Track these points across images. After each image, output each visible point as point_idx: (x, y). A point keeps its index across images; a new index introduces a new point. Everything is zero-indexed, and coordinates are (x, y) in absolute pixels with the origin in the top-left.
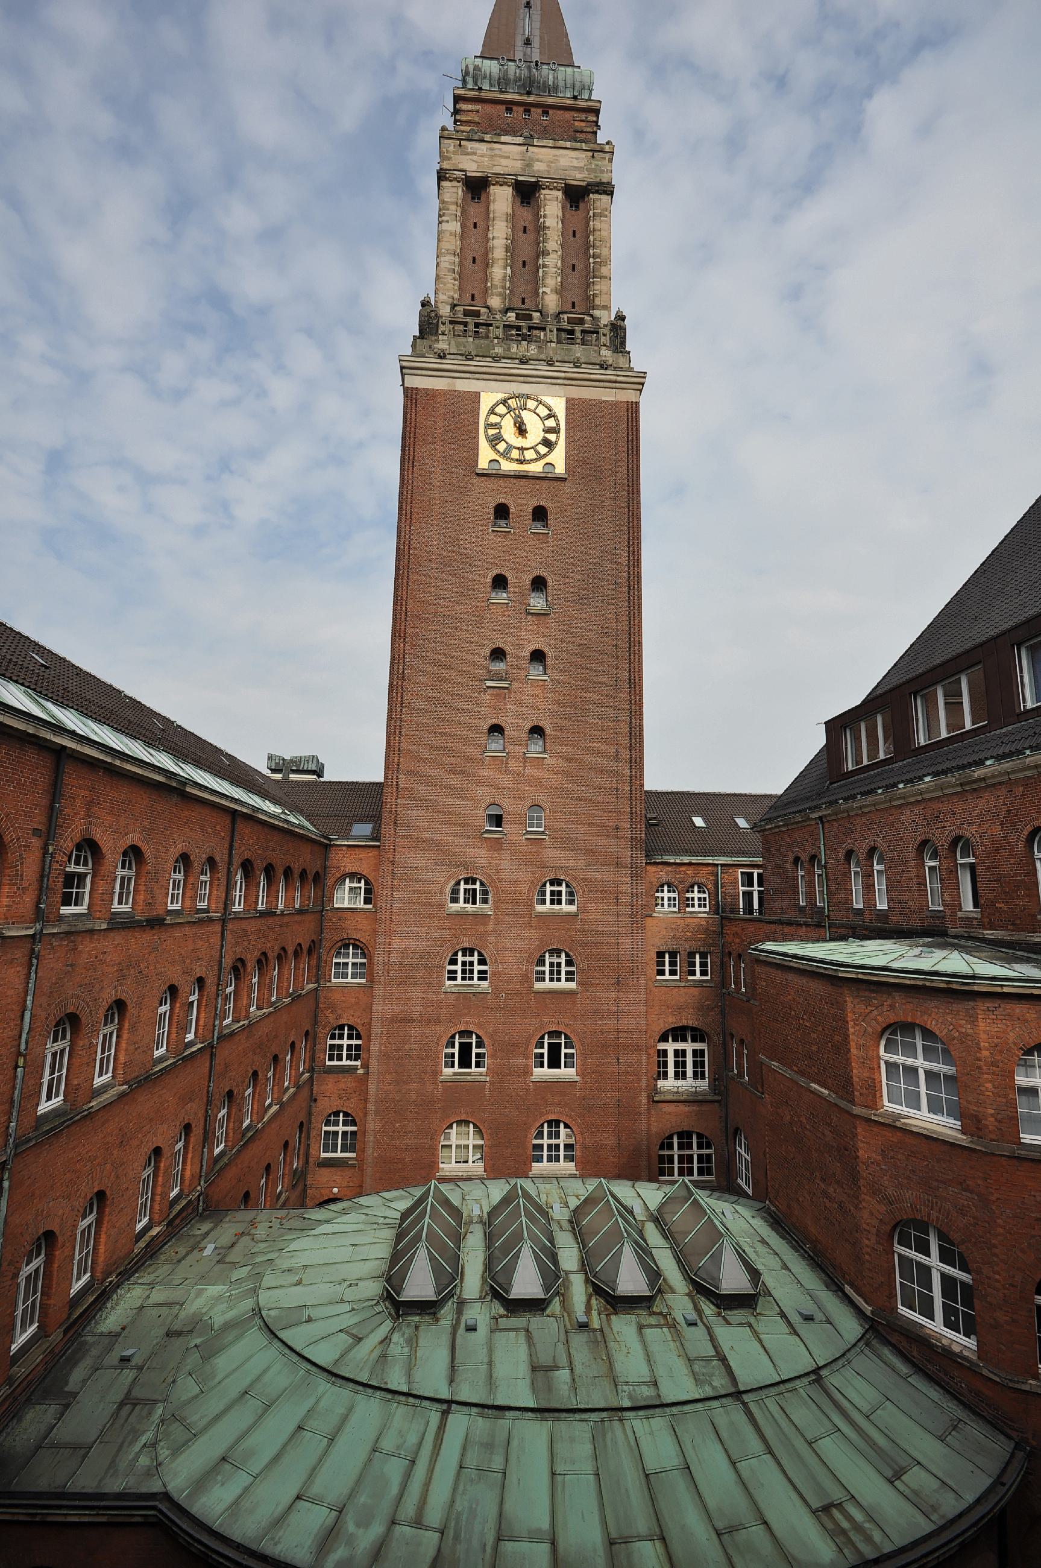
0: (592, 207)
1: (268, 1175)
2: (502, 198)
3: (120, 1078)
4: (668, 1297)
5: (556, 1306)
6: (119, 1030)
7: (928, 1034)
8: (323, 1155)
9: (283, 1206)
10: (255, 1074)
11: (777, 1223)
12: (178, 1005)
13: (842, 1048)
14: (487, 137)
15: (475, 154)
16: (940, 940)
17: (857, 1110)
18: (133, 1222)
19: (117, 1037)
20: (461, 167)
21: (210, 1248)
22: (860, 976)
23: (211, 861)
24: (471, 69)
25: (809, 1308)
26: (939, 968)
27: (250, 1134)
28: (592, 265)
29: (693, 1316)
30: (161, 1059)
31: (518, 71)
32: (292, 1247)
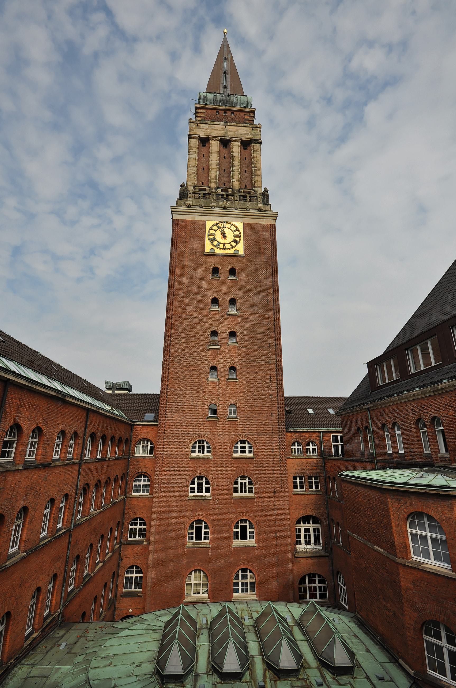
0: (253, 148)
1: (95, 602)
2: (215, 146)
3: (22, 549)
4: (307, 669)
5: (247, 677)
6: (24, 523)
7: (430, 518)
8: (125, 590)
9: (103, 620)
10: (91, 545)
11: (362, 624)
12: (54, 509)
13: (388, 527)
14: (209, 122)
15: (204, 129)
16: (431, 469)
17: (398, 560)
18: (24, 630)
19: (22, 526)
20: (198, 133)
21: (63, 645)
22: (394, 488)
23: (76, 434)
24: (202, 97)
25: (381, 673)
26: (431, 483)
27: (87, 579)
28: (253, 171)
29: (320, 680)
30: (44, 538)
31: (221, 98)
32: (107, 644)
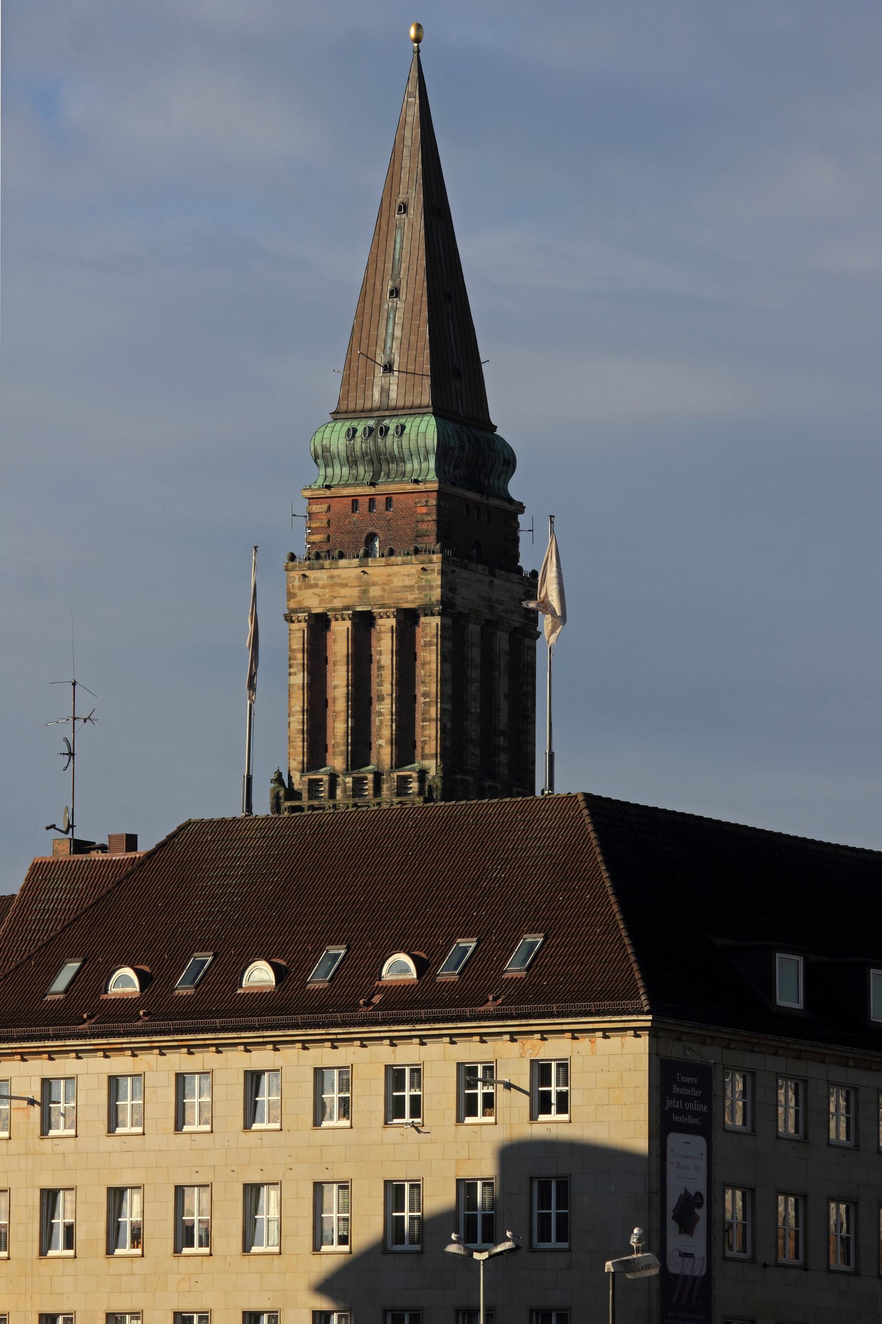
15: (316, 586)
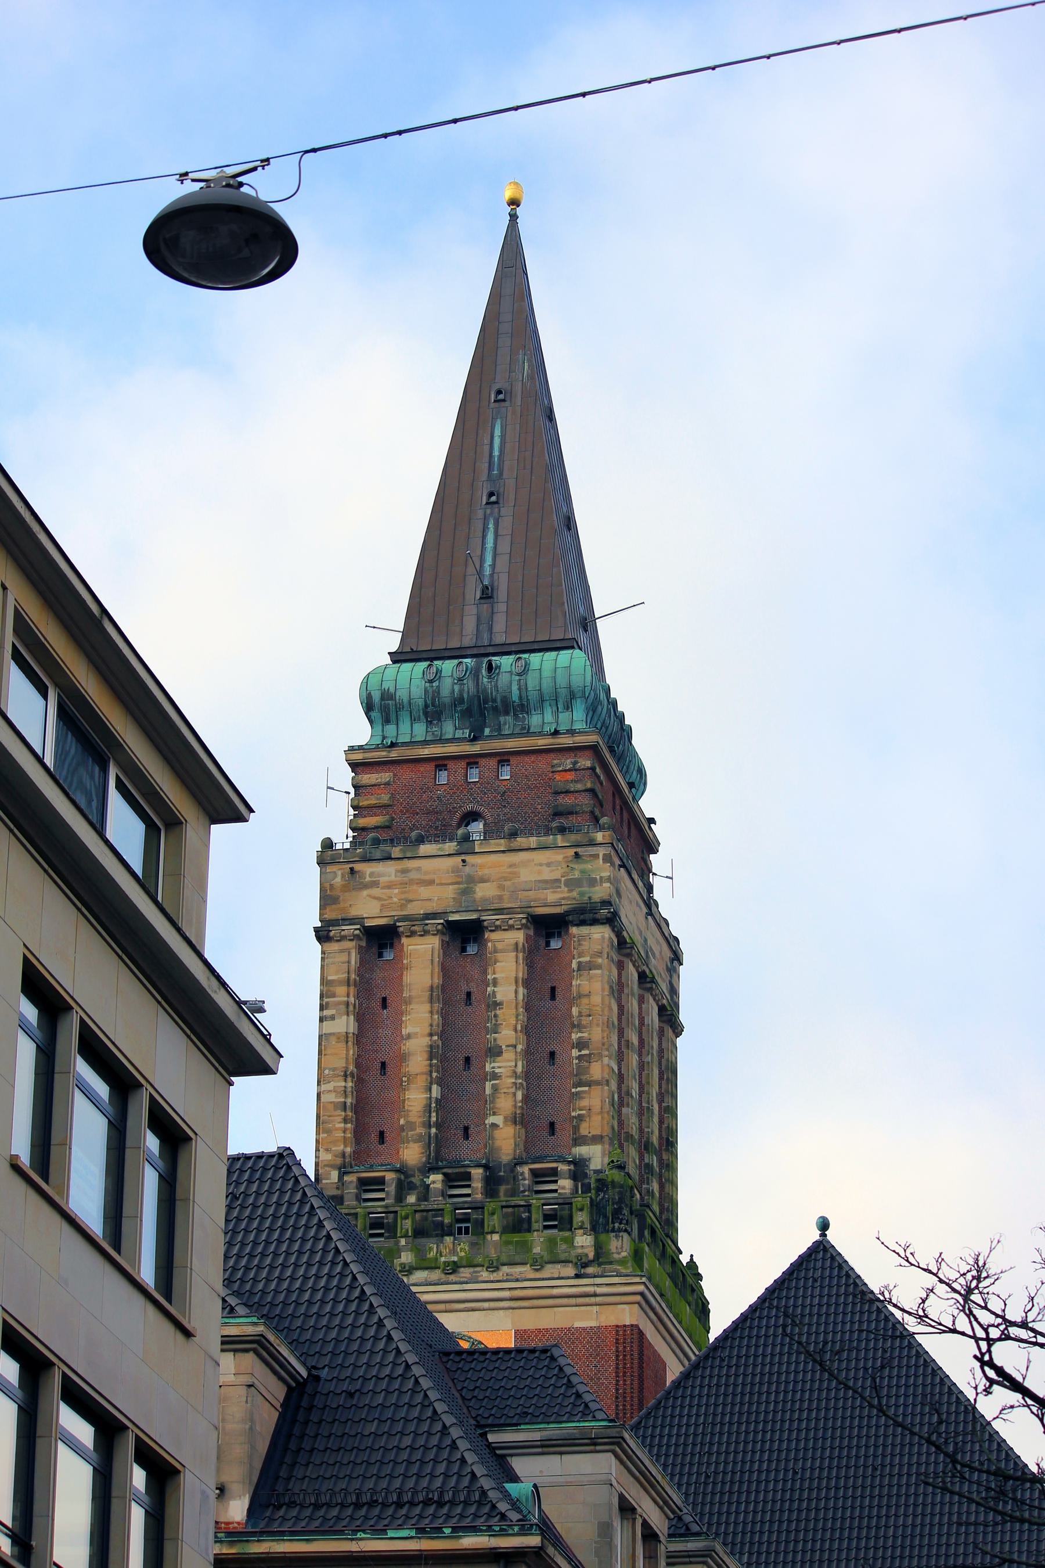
15: (375, 884)
20: (354, 912)
